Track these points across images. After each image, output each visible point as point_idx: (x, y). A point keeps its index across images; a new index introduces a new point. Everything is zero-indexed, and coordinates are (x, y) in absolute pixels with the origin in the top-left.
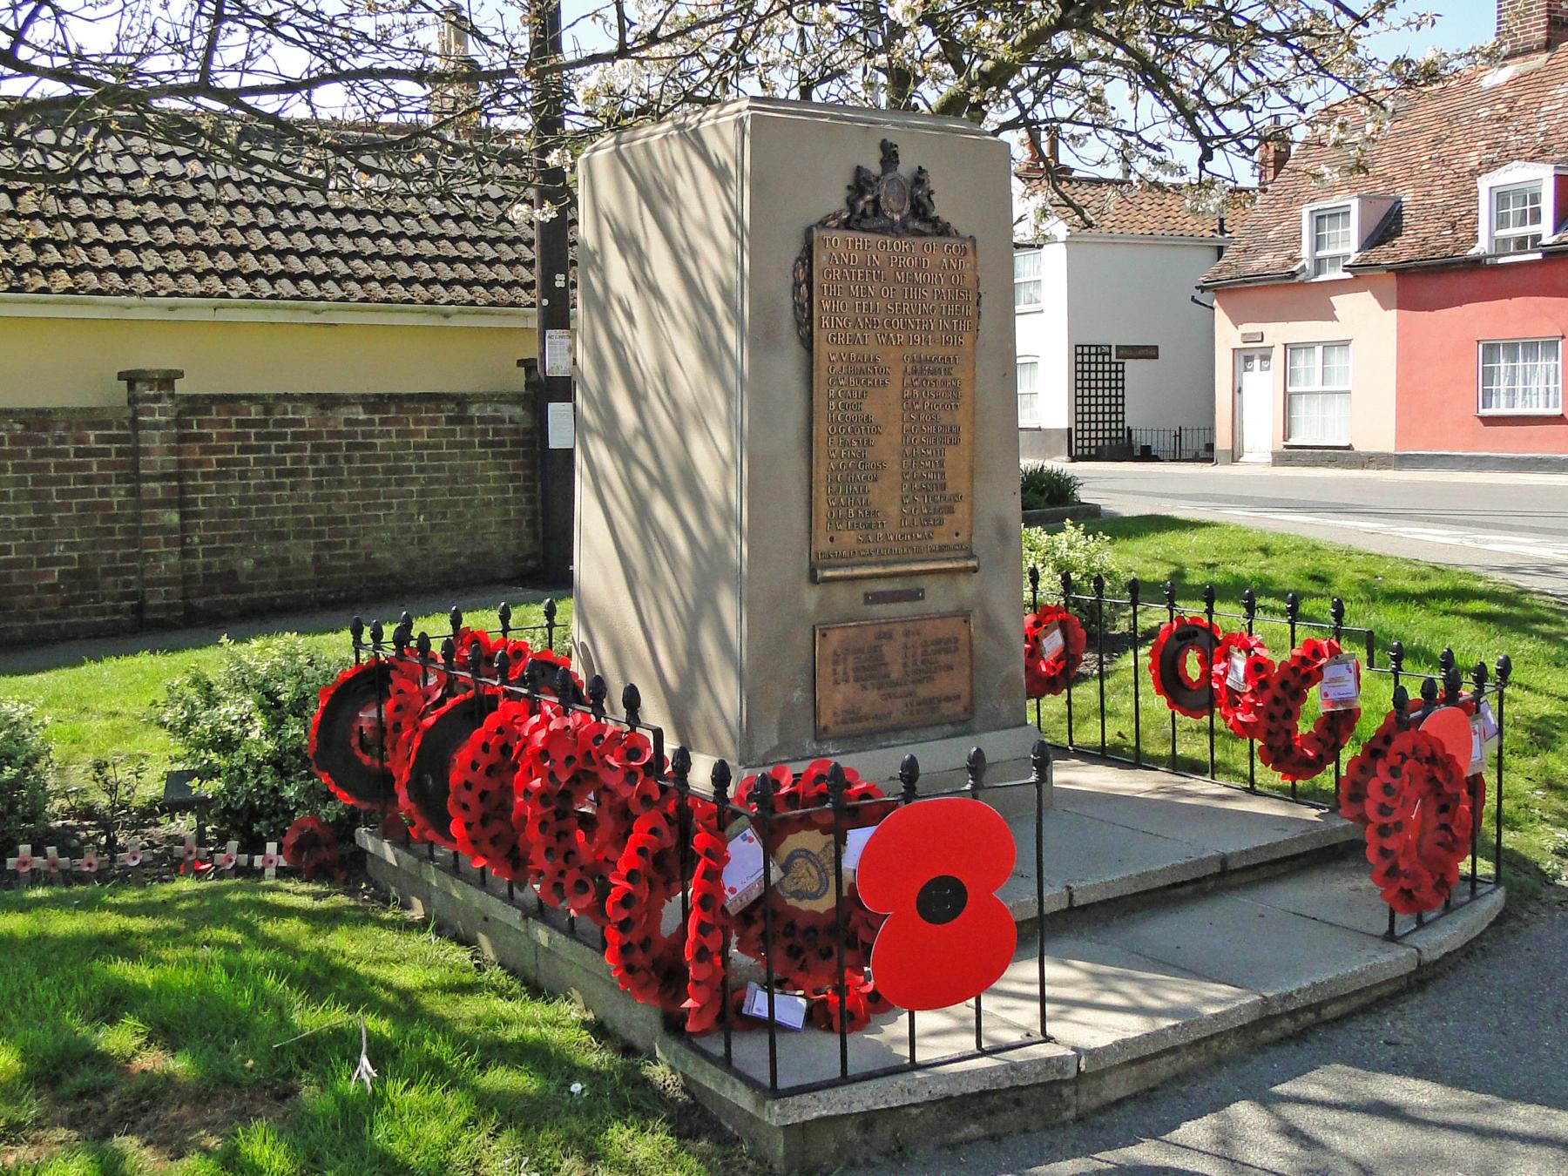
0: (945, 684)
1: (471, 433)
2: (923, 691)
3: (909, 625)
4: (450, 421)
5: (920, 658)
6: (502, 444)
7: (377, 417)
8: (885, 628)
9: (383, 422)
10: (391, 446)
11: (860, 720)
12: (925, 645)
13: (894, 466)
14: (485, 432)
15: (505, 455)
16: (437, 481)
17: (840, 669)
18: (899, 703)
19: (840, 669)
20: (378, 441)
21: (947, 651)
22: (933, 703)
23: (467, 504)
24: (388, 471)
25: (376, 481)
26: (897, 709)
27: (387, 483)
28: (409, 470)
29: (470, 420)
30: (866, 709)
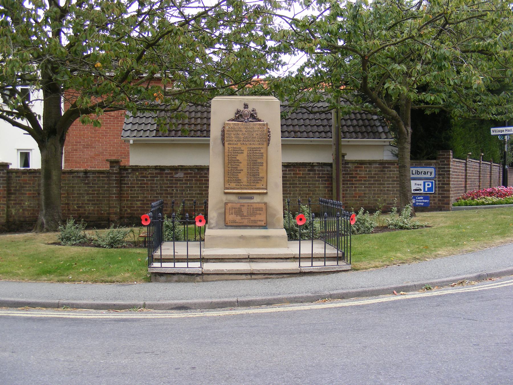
0: (258, 217)
1: (315, 174)
2: (252, 218)
3: (249, 204)
4: (309, 170)
5: (252, 211)
6: (325, 177)
7: (287, 169)
8: (243, 204)
9: (289, 171)
10: (292, 177)
11: (236, 223)
12: (253, 208)
13: (245, 170)
14: (319, 174)
15: (325, 181)
16: (305, 187)
17: (231, 212)
18: (247, 220)
19: (231, 212)
20: (288, 176)
21: (260, 210)
22: (255, 221)
23: (313, 194)
24: (290, 184)
25: (287, 187)
26: (246, 222)
27: (290, 187)
28: (296, 184)
29: (315, 170)
30: (237, 221)
